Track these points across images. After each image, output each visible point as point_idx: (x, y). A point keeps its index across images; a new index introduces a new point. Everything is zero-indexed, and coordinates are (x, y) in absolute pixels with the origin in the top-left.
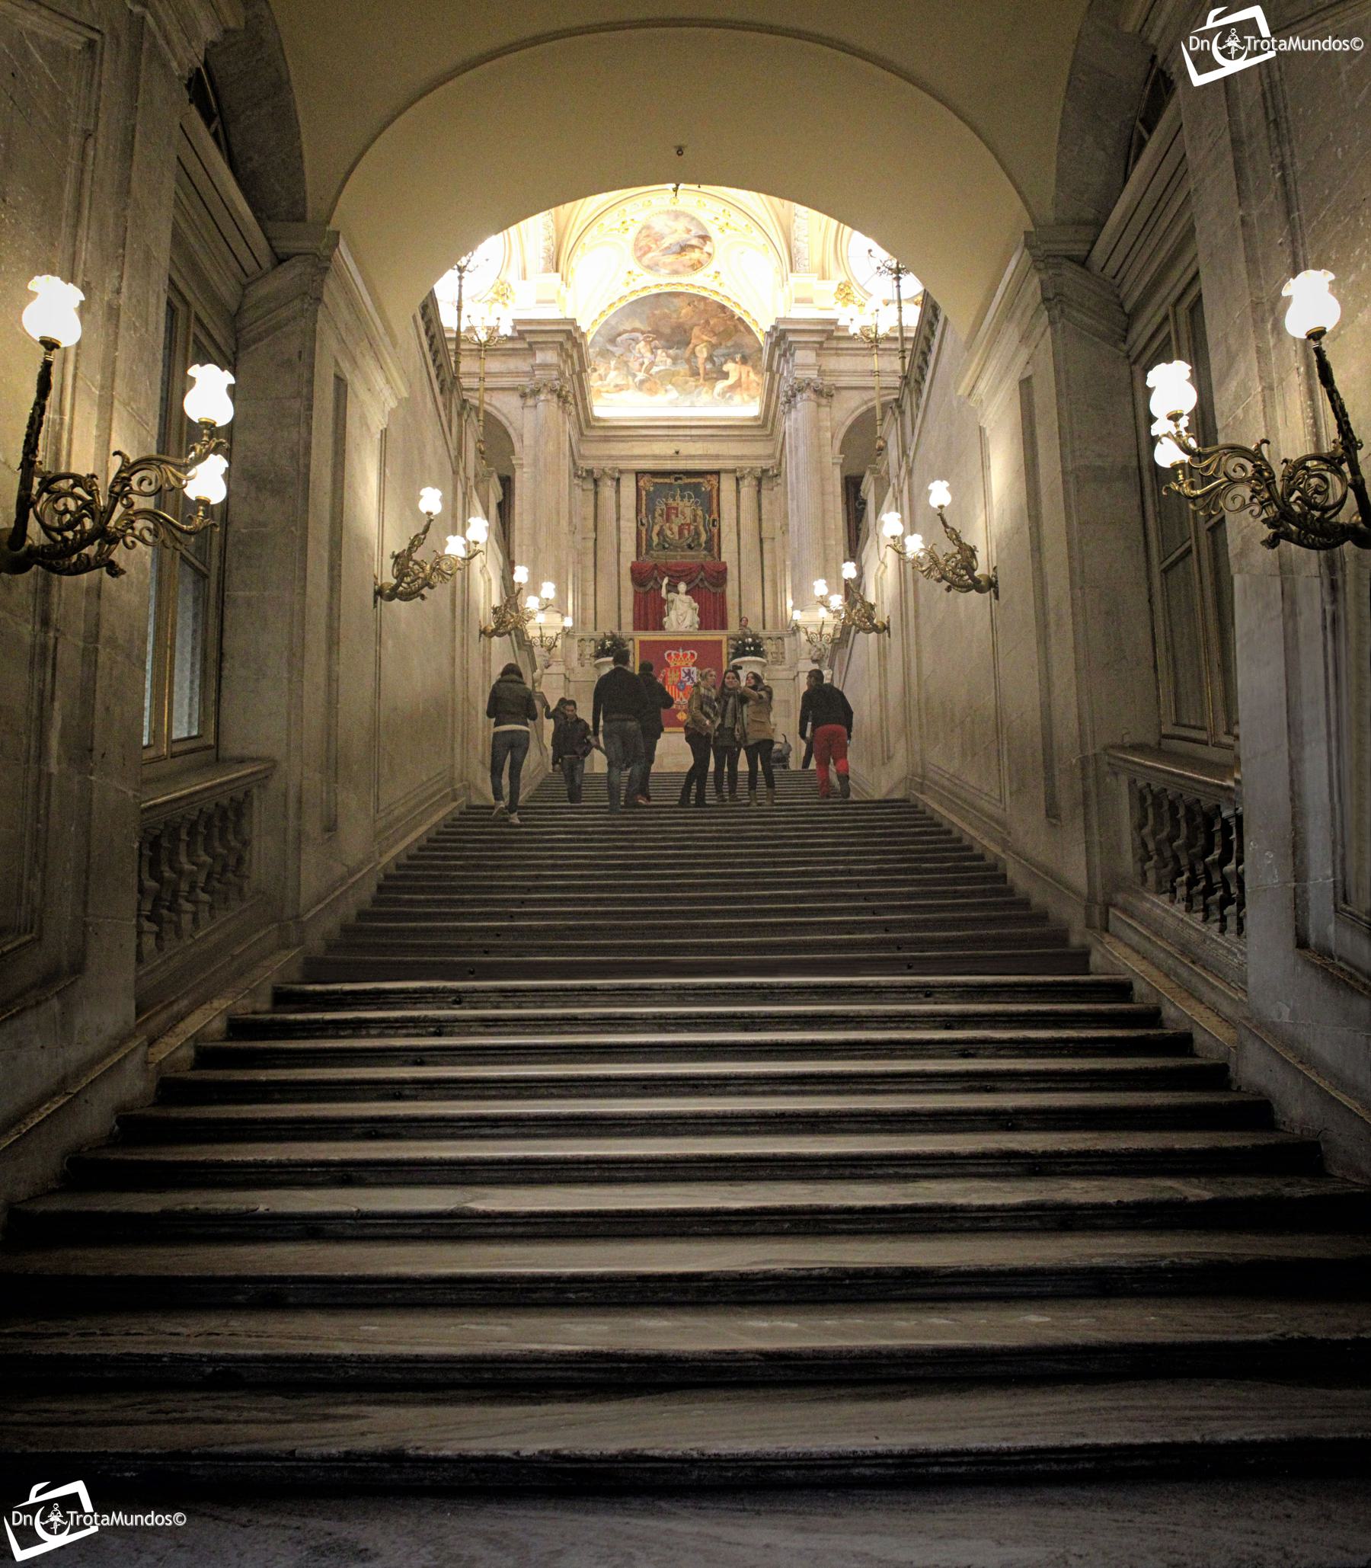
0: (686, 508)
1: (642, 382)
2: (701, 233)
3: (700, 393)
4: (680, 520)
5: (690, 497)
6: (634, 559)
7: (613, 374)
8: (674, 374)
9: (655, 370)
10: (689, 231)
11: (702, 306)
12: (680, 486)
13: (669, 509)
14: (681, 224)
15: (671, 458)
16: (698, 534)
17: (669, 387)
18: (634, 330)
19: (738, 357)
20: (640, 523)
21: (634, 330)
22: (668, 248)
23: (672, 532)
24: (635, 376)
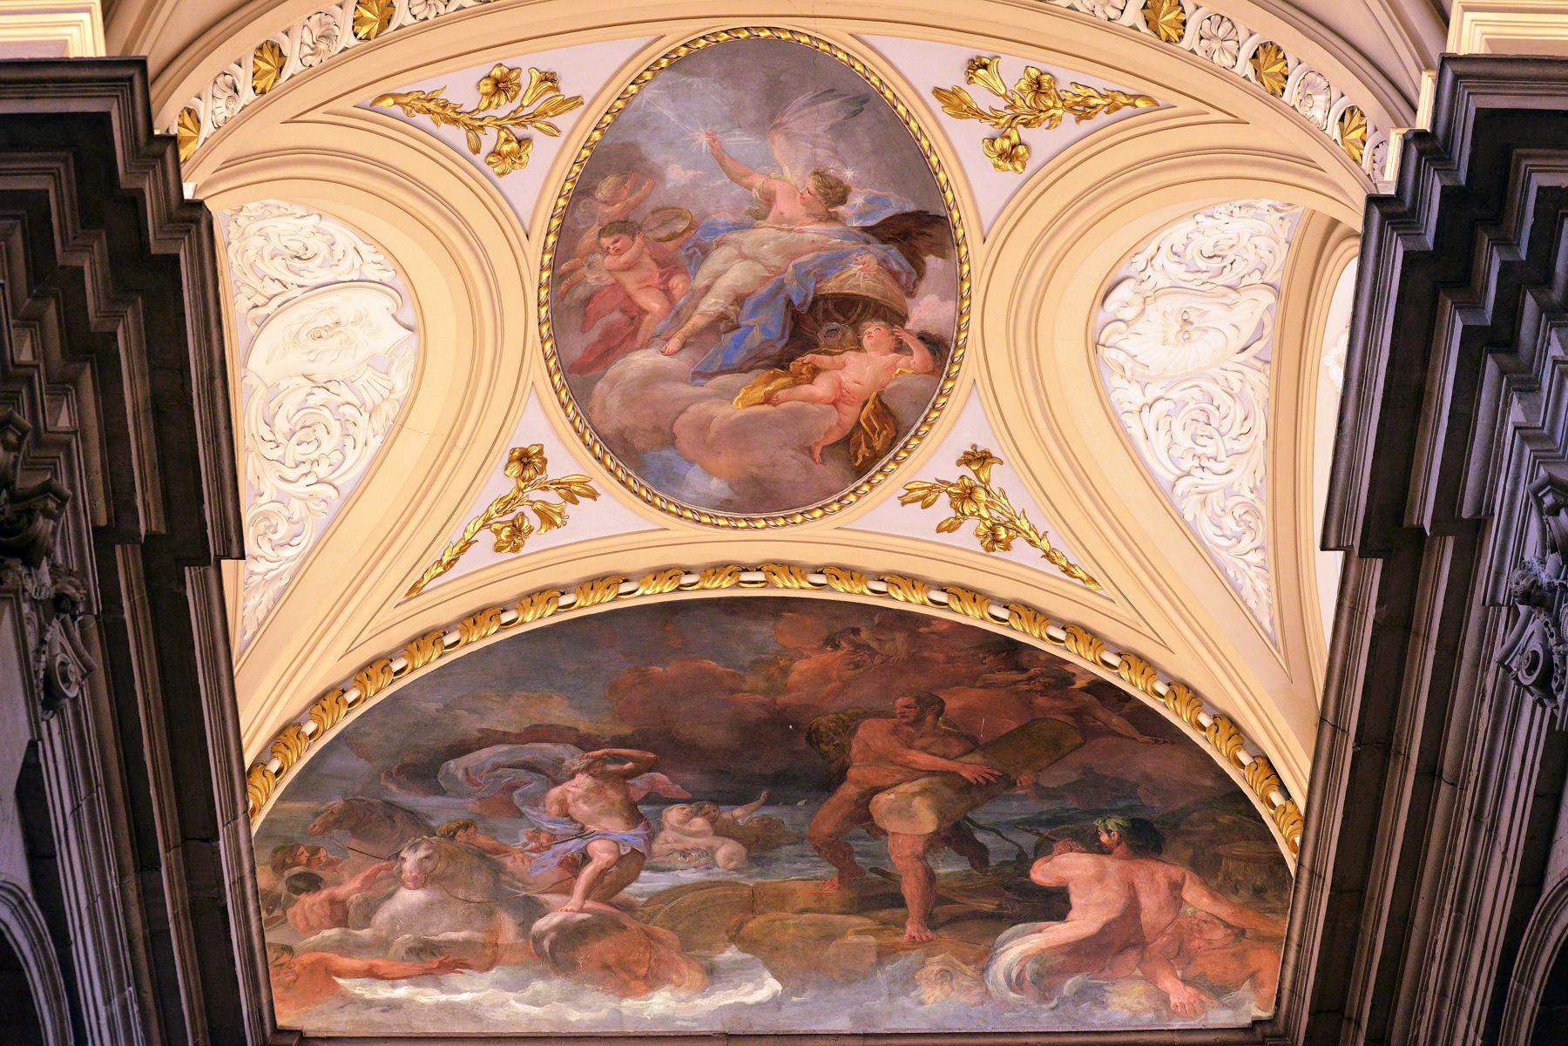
1: (572, 936)
2: (899, 204)
7: (409, 897)
8: (753, 903)
9: (649, 883)
10: (833, 194)
11: (899, 643)
17: (730, 954)
19: (1109, 830)
21: (538, 733)
22: (722, 324)
24: (531, 909)
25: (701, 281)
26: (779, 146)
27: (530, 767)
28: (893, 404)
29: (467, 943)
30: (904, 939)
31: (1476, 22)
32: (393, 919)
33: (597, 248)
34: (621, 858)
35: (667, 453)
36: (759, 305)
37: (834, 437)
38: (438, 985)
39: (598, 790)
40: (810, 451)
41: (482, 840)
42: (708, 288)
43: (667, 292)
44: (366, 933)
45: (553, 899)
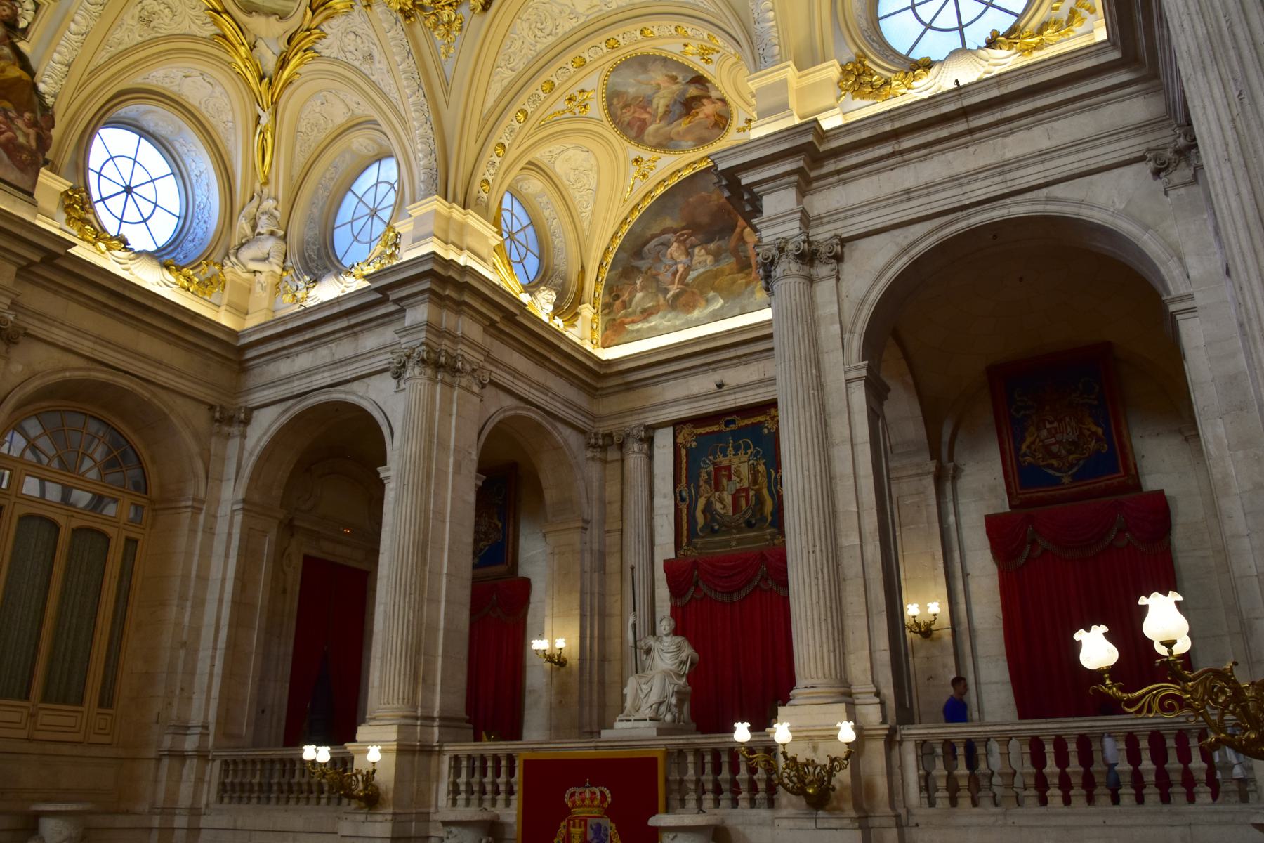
0: (742, 465)
2: (690, 76)
3: (753, 293)
4: (734, 485)
5: (747, 447)
6: (672, 556)
7: (639, 295)
8: (716, 275)
9: (693, 275)
12: (732, 432)
13: (718, 470)
14: (658, 76)
15: (712, 395)
16: (760, 501)
17: (712, 294)
18: (665, 231)
20: (679, 498)
21: (665, 231)
22: (666, 113)
23: (724, 504)
24: (666, 291)
25: (654, 106)
26: (652, 74)
27: (663, 244)
28: (721, 113)
29: (653, 307)
30: (751, 279)
31: (752, 84)
32: (636, 304)
33: (622, 113)
34: (685, 269)
35: (673, 142)
36: (673, 106)
37: (712, 124)
38: (647, 322)
39: (679, 247)
40: (708, 128)
41: (654, 272)
42: (658, 108)
43: (648, 113)
44: (630, 310)
45: (670, 287)
